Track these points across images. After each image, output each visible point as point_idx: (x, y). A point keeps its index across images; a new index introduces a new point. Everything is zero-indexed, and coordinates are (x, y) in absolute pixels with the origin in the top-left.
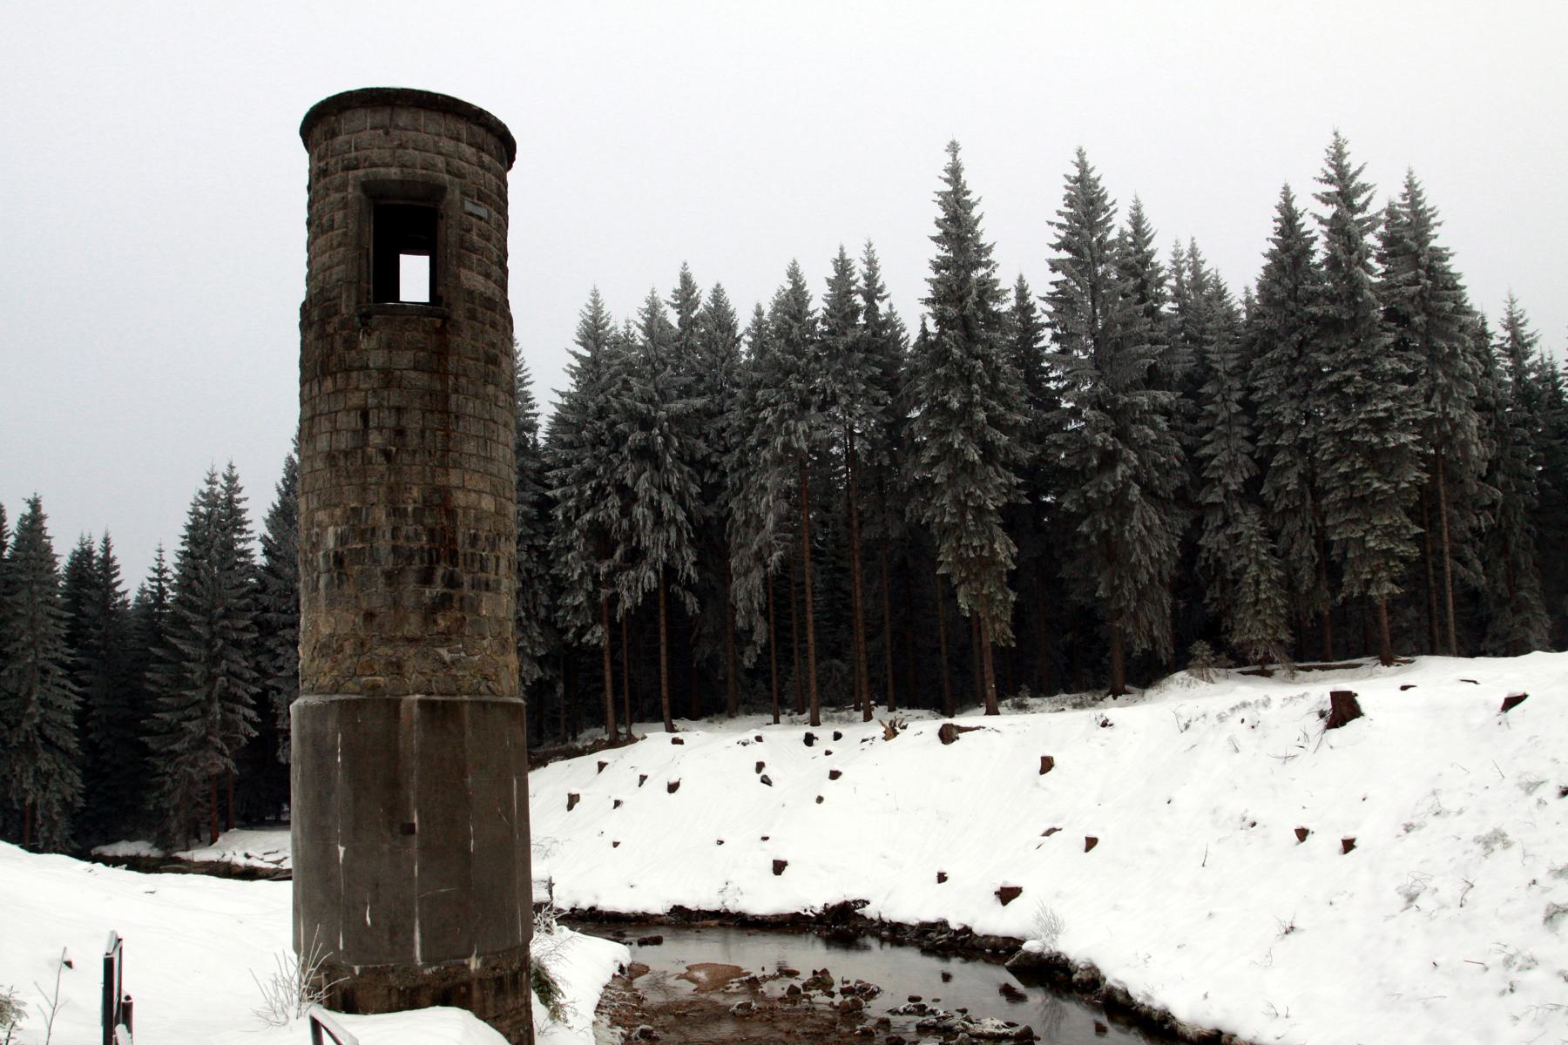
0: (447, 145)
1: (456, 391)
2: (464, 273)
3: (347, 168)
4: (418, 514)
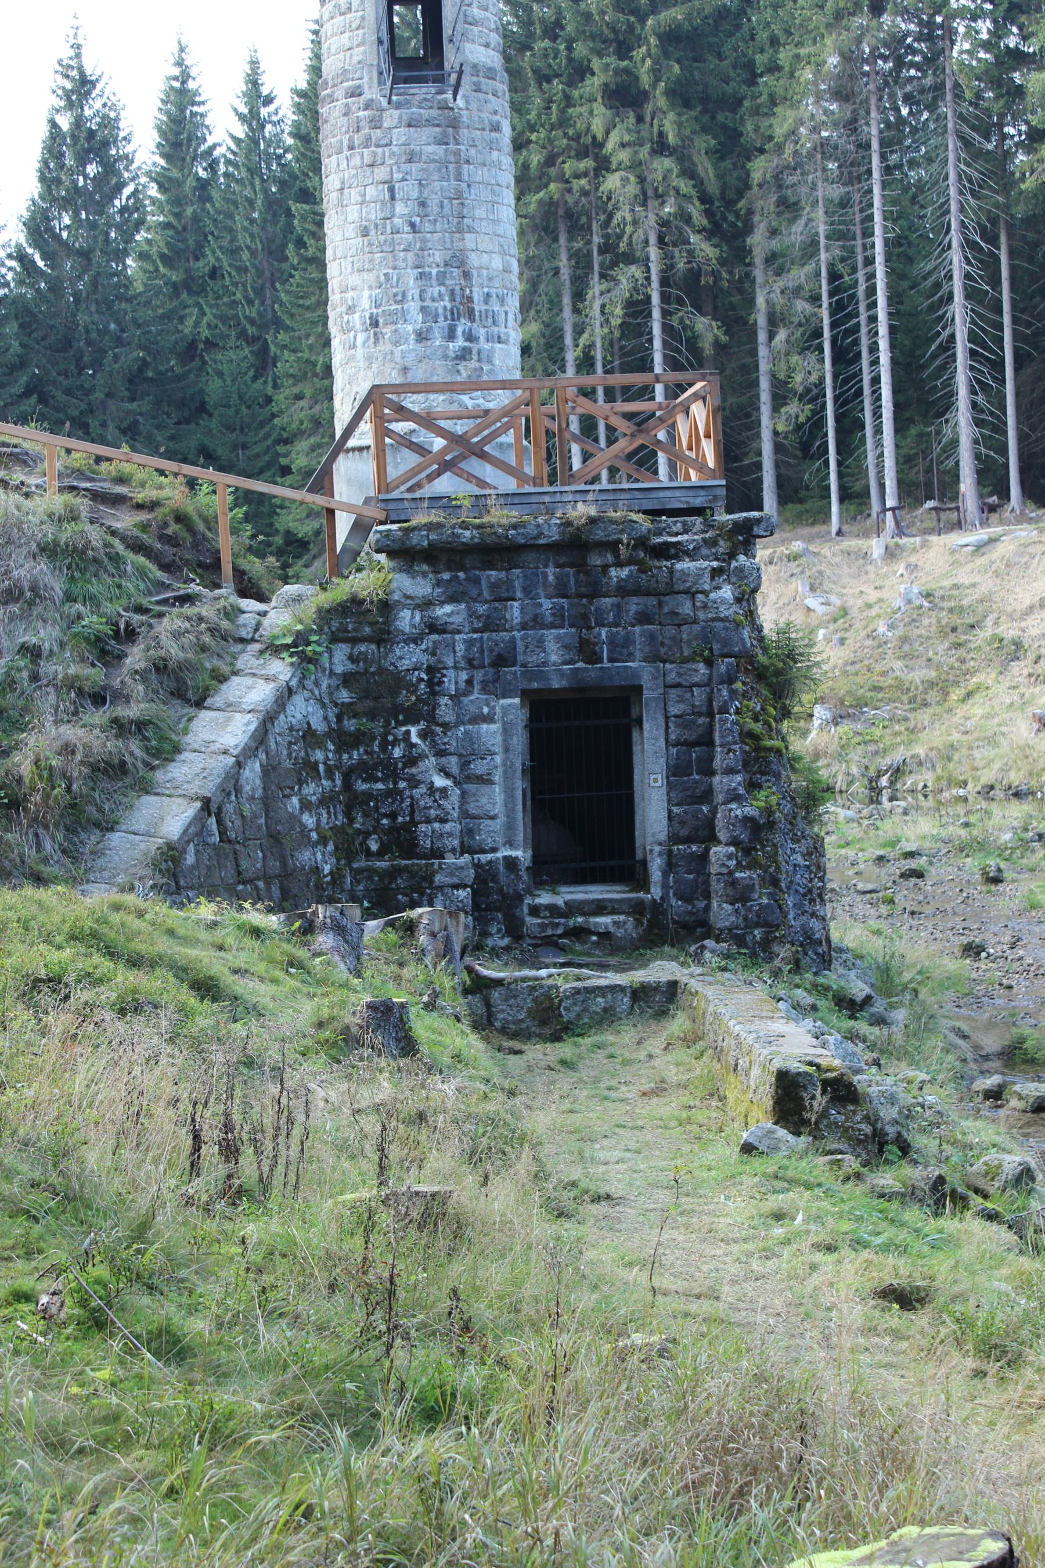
1: (468, 162)
2: (468, 46)
4: (441, 279)
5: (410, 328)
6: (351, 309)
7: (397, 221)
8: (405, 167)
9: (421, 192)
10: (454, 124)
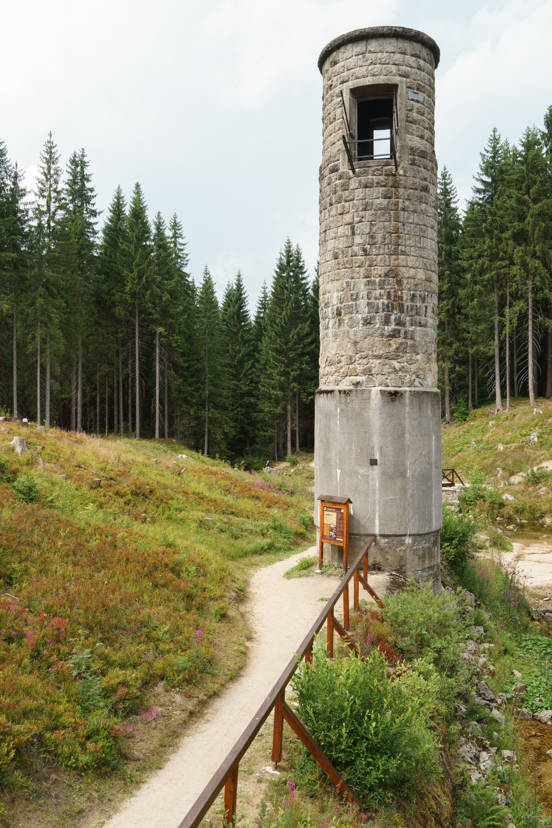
0: (398, 56)
1: (403, 210)
3: (342, 82)
5: (360, 316)
6: (327, 305)
7: (355, 248)
8: (361, 213)
9: (370, 229)
10: (396, 186)
